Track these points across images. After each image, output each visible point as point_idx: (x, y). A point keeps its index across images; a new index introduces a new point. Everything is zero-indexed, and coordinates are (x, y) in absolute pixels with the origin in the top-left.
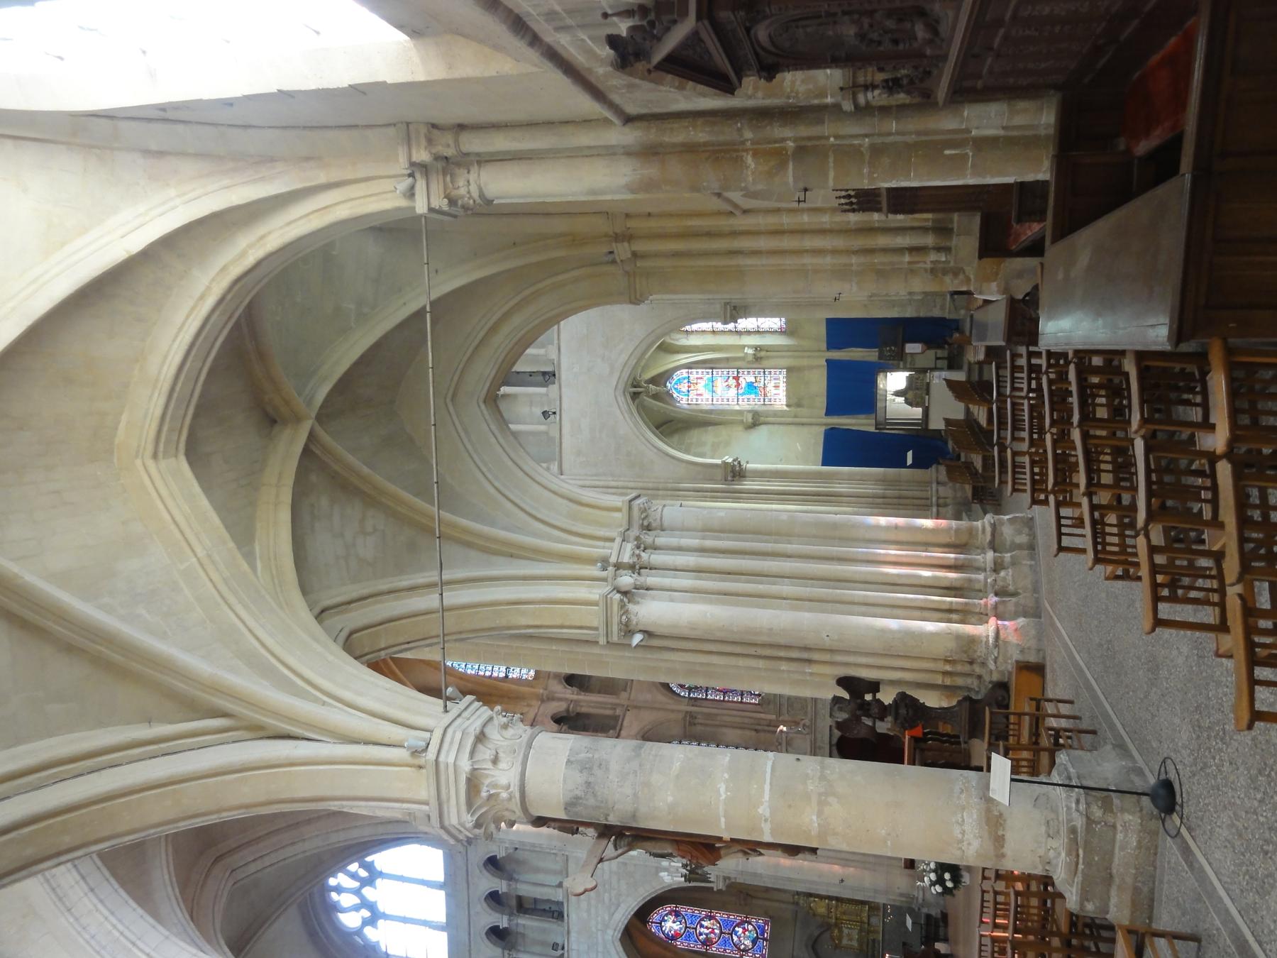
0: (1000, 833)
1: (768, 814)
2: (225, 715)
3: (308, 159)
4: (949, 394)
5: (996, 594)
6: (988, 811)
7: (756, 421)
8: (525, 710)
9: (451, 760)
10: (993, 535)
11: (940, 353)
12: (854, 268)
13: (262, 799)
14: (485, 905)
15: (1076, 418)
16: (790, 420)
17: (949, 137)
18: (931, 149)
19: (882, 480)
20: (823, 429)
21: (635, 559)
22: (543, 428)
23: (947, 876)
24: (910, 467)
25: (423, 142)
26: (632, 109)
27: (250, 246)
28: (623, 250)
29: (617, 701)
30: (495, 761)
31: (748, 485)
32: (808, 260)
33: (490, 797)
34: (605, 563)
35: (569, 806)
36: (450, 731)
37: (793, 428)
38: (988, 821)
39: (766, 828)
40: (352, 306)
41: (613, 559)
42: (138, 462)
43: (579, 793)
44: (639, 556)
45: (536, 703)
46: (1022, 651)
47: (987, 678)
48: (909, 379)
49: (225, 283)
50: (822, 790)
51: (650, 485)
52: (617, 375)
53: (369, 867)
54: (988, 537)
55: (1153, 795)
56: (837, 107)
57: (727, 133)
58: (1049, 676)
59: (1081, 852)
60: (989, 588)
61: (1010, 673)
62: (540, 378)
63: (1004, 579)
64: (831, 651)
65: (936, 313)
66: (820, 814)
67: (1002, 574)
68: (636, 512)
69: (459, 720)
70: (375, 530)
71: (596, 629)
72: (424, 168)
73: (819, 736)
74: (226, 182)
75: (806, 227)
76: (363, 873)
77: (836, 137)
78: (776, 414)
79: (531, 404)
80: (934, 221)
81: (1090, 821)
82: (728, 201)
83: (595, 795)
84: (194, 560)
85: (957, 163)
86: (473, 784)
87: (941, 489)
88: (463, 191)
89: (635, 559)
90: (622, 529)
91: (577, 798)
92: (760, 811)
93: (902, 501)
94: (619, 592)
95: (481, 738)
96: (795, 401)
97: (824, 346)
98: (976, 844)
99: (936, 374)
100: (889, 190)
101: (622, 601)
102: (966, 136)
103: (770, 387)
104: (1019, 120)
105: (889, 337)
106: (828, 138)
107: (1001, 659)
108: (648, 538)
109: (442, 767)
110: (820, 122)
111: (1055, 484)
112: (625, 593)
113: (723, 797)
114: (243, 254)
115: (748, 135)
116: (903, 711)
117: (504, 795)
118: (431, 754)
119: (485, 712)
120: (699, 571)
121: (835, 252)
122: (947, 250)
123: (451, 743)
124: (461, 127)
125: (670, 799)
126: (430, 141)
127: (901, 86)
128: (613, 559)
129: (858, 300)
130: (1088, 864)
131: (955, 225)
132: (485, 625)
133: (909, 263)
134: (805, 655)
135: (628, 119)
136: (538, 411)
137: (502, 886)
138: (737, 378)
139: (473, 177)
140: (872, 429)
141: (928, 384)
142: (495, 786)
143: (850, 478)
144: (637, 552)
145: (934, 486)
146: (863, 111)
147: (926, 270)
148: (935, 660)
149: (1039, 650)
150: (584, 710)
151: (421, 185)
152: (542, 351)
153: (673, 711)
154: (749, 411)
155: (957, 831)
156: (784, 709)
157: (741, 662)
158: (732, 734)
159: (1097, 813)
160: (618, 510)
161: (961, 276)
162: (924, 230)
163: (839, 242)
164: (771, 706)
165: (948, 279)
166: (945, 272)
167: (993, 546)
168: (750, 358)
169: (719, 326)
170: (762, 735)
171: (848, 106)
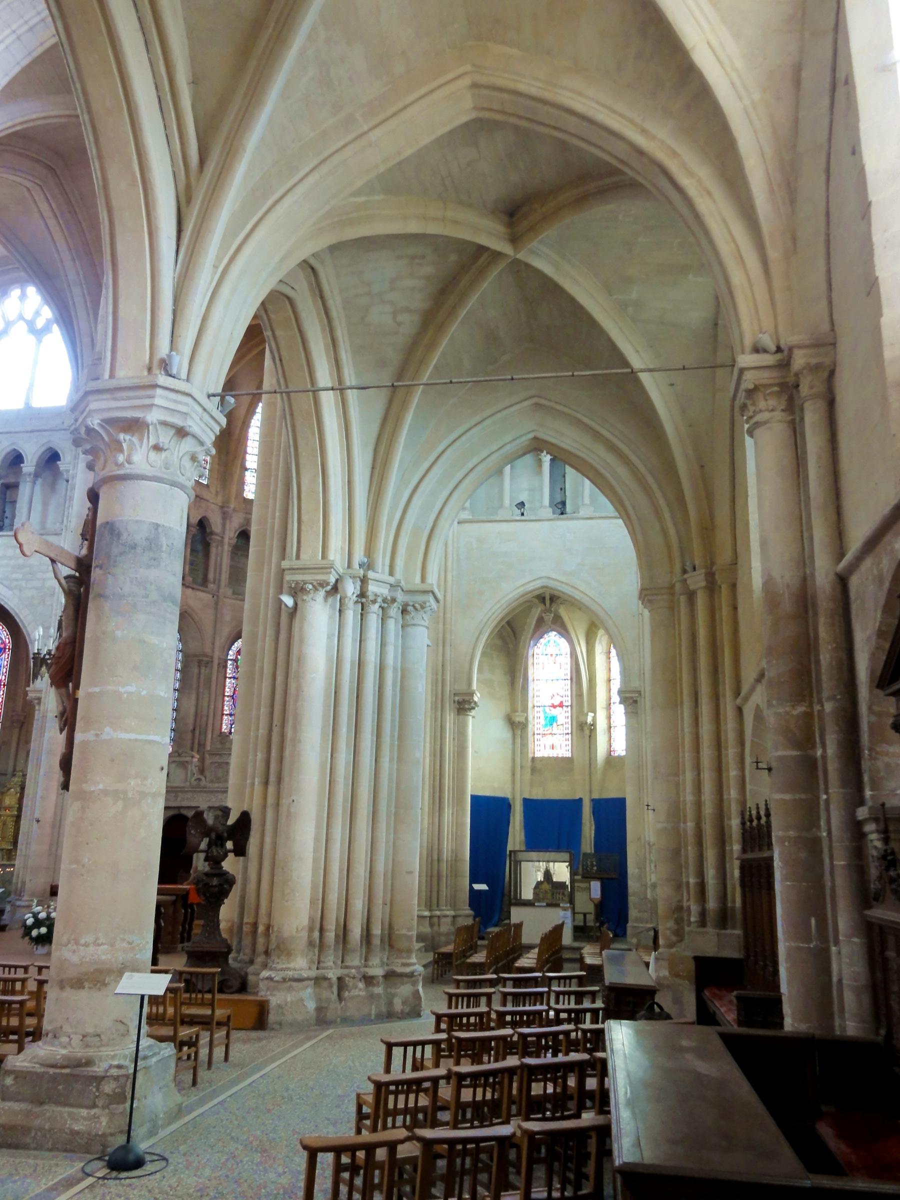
0: (87, 985)
1: (104, 737)
2: (202, 162)
3: (794, 239)
4: (548, 928)
5: (340, 979)
6: (109, 972)
7: (517, 726)
8: (213, 490)
9: (157, 401)
10: (402, 975)
11: (591, 918)
12: (682, 825)
13: (115, 203)
14: (9, 449)
15: (529, 1061)
16: (518, 760)
17: (830, 921)
18: (814, 903)
19: (456, 859)
20: (509, 796)
21: (371, 598)
22: (507, 502)
23: (43, 930)
24: (471, 888)
25: (814, 361)
26: (854, 582)
27: (699, 181)
28: (697, 581)
29: (223, 584)
30: (157, 448)
31: (450, 718)
32: (689, 776)
33: (119, 443)
34: (369, 566)
35: (110, 526)
36: (189, 400)
37: (510, 765)
38: (100, 971)
39: (90, 736)
40: (634, 296)
41: (371, 574)
42: (468, 68)
43: (124, 537)
44: (374, 602)
46: (279, 1006)
47: (251, 969)
48: (562, 885)
49: (660, 155)
50: (130, 795)
51: (448, 615)
52: (563, 579)
53: (46, 329)
54: (400, 970)
55: (126, 1148)
56: (861, 802)
57: (828, 683)
58: (254, 1034)
59: (67, 1071)
60: (346, 971)
61: (256, 994)
62: (559, 499)
63: (356, 987)
64: (277, 805)
65: (633, 913)
66: (105, 792)
67: (361, 985)
68: (420, 598)
69: (200, 410)
70: (399, 324)
71: (298, 557)
72: (784, 365)
73: (189, 795)
74: (769, 152)
75: (724, 775)
76: (40, 323)
77: (827, 802)
78: (524, 745)
79: (531, 490)
80: (733, 909)
81: (99, 1080)
82: (752, 689)
83: (121, 554)
84: (366, 128)
85: (800, 931)
86: (135, 426)
87: (449, 920)
88: (762, 404)
89: (371, 598)
90: (403, 584)
91: (119, 535)
92: (107, 729)
94: (337, 581)
95: (181, 433)
96: (538, 766)
97: (596, 796)
98: (75, 959)
99: (569, 913)
100: (771, 859)
101: (328, 584)
102: (831, 939)
104: (849, 997)
105: (607, 865)
106: (827, 793)
107: (272, 984)
108: (394, 611)
109: (149, 392)
110: (844, 785)
111: (457, 1038)
112: (335, 589)
113: (121, 690)
114: (691, 174)
115: (828, 707)
116: (215, 881)
117: (121, 458)
118: (162, 380)
119: (209, 439)
120: (361, 665)
121: (699, 805)
122: (703, 923)
123: (175, 401)
124: (831, 403)
125: (119, 633)
126: (815, 369)
127: (887, 869)
128: (371, 574)
129: (644, 832)
130: (54, 1079)
131: (728, 931)
132: (300, 441)
133: (688, 883)
134: (272, 778)
135: (842, 581)
136: (523, 497)
137: (28, 467)
138: (561, 705)
139: (778, 415)
140: (510, 847)
141: (557, 905)
142: (132, 447)
143: (458, 825)
144: (380, 600)
145: (452, 913)
146: (856, 830)
147: (681, 901)
148: (269, 915)
149: (280, 1024)
150: (213, 550)
151: (769, 359)
152: (587, 500)
153: (213, 644)
154: (527, 719)
155: (89, 938)
156: (217, 759)
157: (264, 710)
158: (190, 705)
159: (108, 1088)
160: (423, 579)
161: (674, 938)
162: (723, 897)
163: (708, 809)
164: (219, 746)
165: (671, 924)
166: (679, 921)
167: (390, 976)
168: (582, 719)
169: (616, 685)
170: (189, 736)
171: (862, 813)
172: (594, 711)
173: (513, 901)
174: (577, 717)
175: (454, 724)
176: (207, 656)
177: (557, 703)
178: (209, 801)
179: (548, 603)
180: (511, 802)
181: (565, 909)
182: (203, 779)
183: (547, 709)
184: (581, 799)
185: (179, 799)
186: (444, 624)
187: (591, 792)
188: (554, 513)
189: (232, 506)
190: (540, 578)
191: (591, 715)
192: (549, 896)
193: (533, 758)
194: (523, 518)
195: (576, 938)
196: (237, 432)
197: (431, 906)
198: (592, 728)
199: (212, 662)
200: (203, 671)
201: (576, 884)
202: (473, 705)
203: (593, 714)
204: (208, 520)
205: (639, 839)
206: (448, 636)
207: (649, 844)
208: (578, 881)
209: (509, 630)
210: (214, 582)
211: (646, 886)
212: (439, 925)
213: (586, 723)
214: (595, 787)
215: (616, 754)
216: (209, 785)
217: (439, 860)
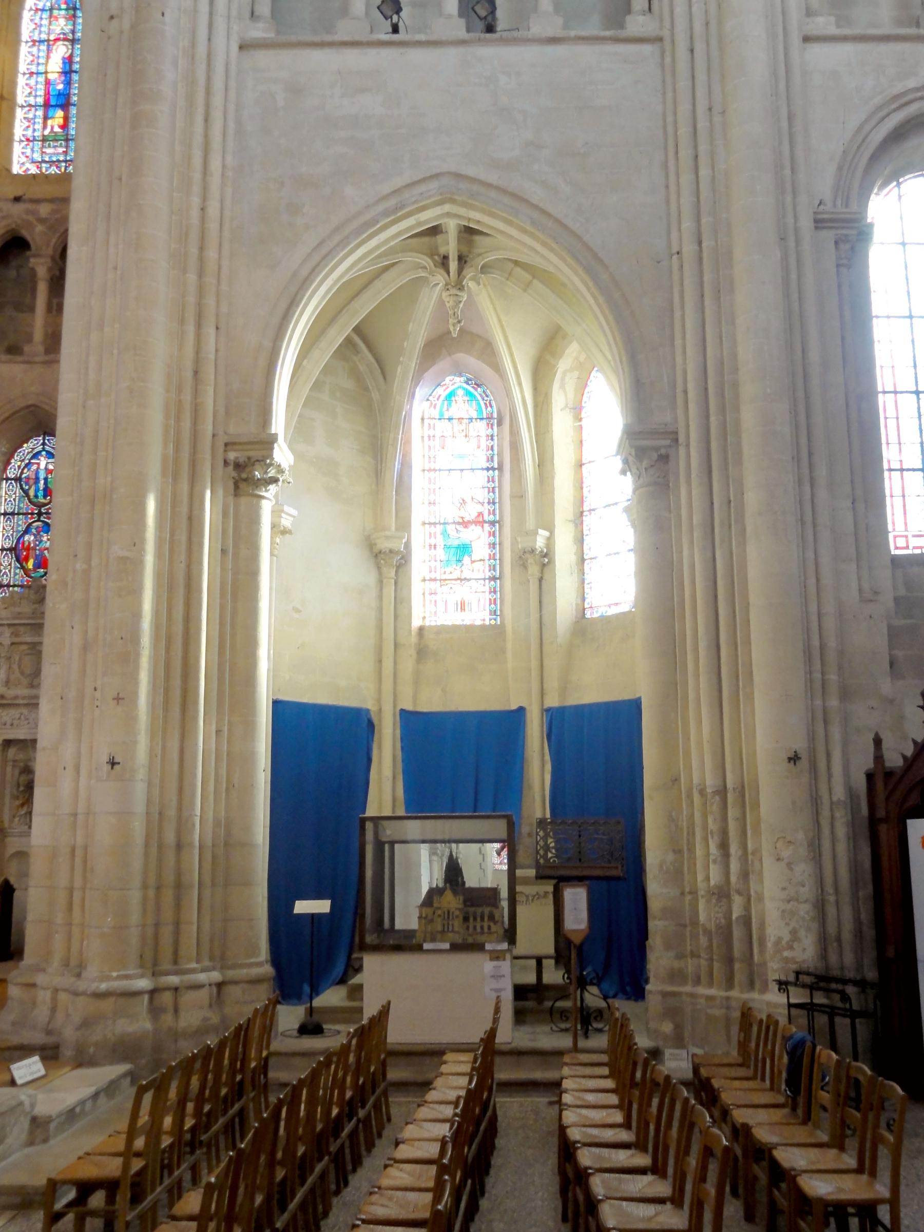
7: (388, 561)
16: (389, 632)
19: (227, 842)
20: (369, 704)
48: (489, 896)
51: (211, 254)
65: (658, 959)
78: (402, 602)
93: (168, 896)
97: (553, 702)
103: (461, 592)
138: (479, 521)
140: (371, 812)
141: (478, 947)
145: (216, 976)
154: (408, 545)
172: (551, 530)
173: (370, 939)
174: (514, 542)
175: (225, 514)
177: (471, 515)
179: (453, 265)
180: (376, 722)
181: (497, 956)
183: (451, 529)
184: (521, 710)
186: (201, 274)
187: (542, 694)
188: (468, 30)
190: (436, 176)
191: (543, 533)
192: (457, 924)
193: (421, 629)
194: (395, 37)
195: (520, 1016)
197: (155, 963)
198: (546, 559)
201: (519, 888)
202: (272, 473)
203: (547, 534)
205: (676, 780)
206: (210, 301)
207: (702, 792)
208: (526, 881)
209: (372, 360)
211: (694, 892)
212: (176, 1011)
213: (533, 551)
214: (552, 683)
215: (596, 615)
217: (179, 846)
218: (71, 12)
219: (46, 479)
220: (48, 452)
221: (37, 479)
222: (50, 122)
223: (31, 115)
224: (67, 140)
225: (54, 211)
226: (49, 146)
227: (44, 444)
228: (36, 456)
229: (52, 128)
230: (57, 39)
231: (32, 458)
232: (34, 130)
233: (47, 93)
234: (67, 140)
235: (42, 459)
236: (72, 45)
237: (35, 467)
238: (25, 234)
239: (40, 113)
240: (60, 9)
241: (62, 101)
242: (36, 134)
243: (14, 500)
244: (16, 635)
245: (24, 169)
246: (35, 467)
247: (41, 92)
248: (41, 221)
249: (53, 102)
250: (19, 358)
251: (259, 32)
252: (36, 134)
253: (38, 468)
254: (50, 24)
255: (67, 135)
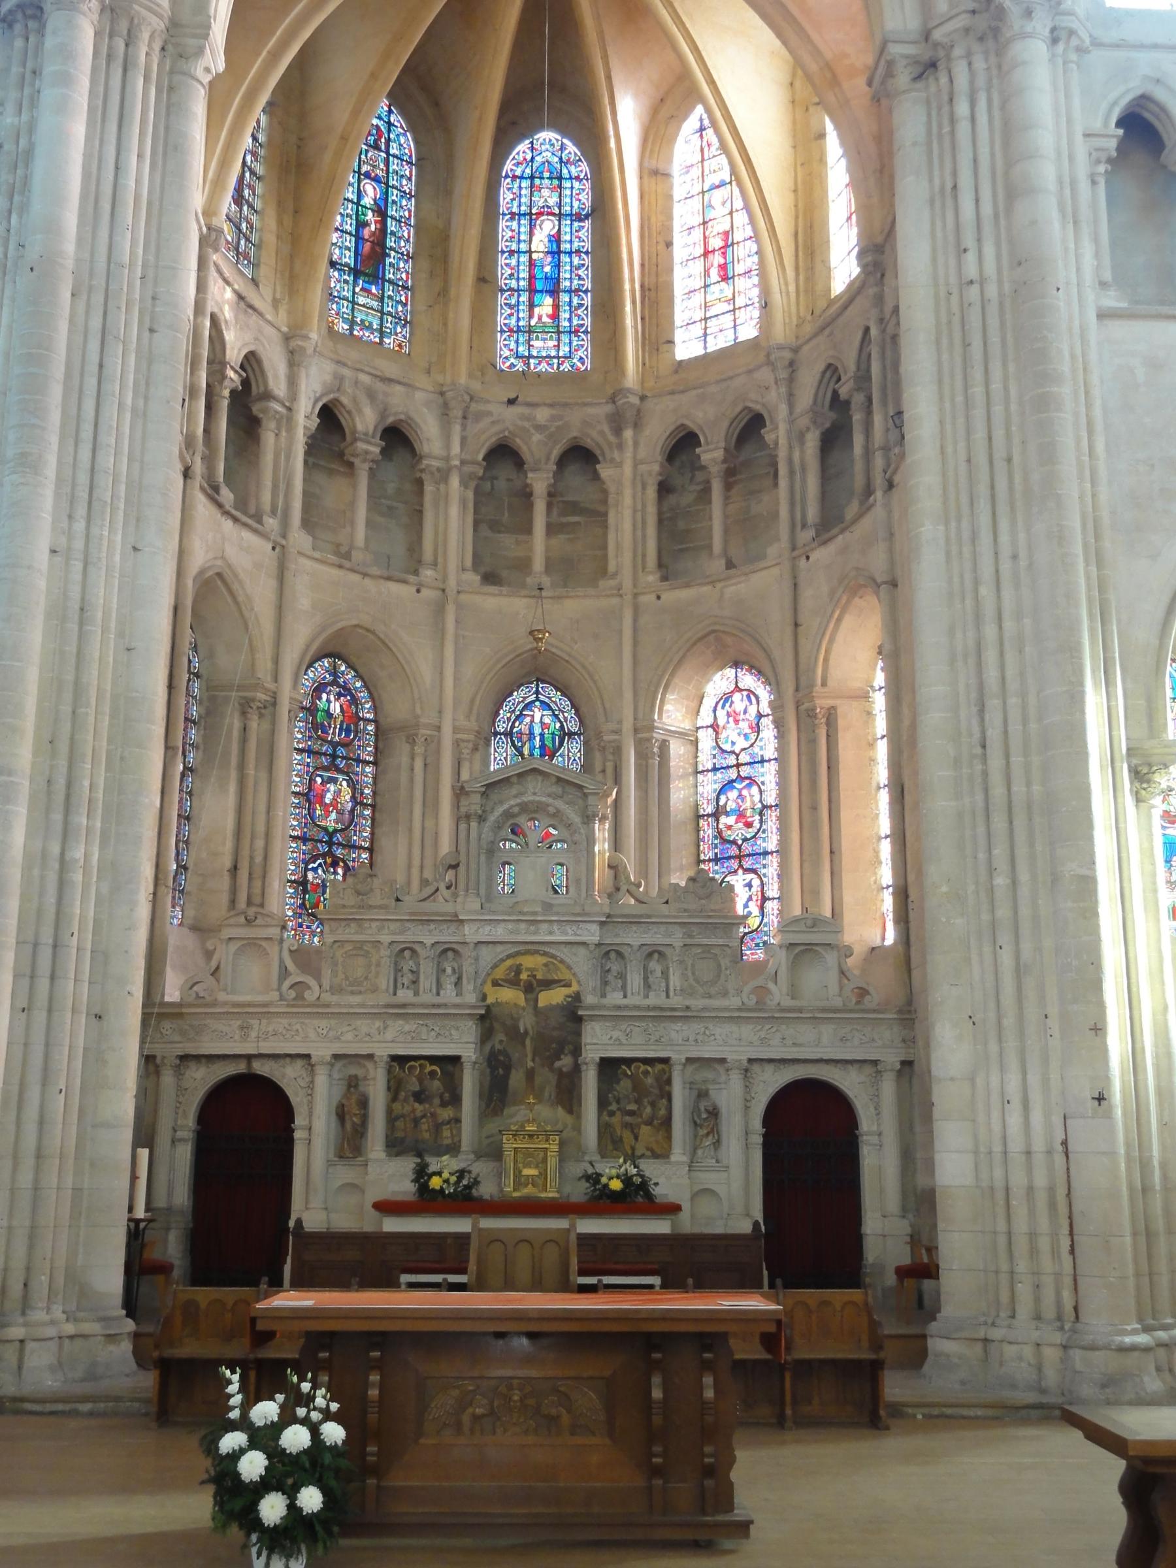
45: (282, 319)
150: (268, 438)
153: (276, 661)
156: (350, 933)
158: (218, 809)
176: (266, 690)
178: (338, 1038)
182: (312, 983)
185: (253, 1034)
189: (314, 336)
196: (328, 157)
199: (274, 704)
200: (254, 724)
204: (259, 362)
210: (274, 512)
216: (327, 997)
218: (556, 182)
219: (542, 735)
220: (542, 702)
221: (531, 734)
222: (537, 310)
223: (513, 301)
224: (559, 332)
225: (553, 418)
226: (537, 338)
227: (537, 692)
228: (528, 706)
229: (540, 318)
230: (540, 214)
231: (526, 707)
232: (518, 319)
233: (532, 278)
234: (559, 332)
235: (536, 710)
236: (559, 221)
237: (528, 720)
238: (519, 443)
239: (524, 298)
240: (541, 178)
241: (550, 287)
242: (521, 324)
243: (506, 759)
244: (690, 936)
245: (508, 364)
246: (528, 720)
247: (524, 274)
248: (539, 428)
249: (539, 285)
250: (524, 592)
251: (1112, 300)
252: (521, 324)
253: (532, 721)
254: (531, 195)
255: (558, 326)
